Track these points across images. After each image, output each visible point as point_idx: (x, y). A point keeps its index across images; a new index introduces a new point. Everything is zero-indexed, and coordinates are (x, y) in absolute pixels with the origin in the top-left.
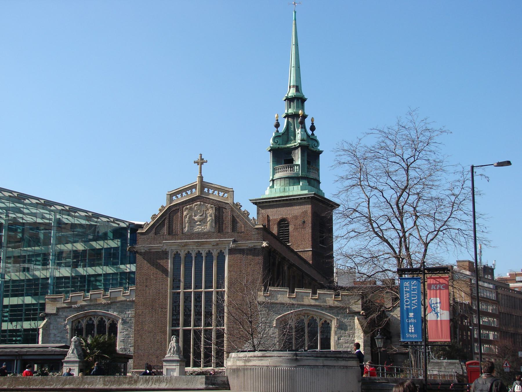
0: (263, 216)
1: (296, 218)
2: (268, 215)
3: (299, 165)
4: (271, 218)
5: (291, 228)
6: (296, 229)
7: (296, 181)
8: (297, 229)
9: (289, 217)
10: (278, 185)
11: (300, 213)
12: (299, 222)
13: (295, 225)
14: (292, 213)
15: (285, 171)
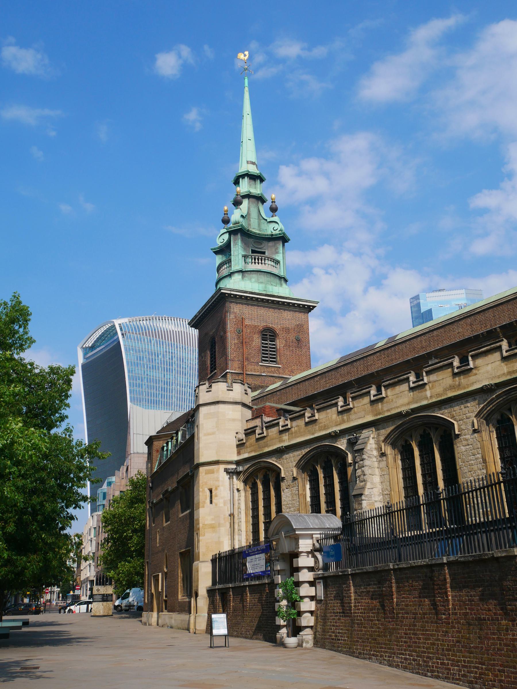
0: (236, 317)
1: (287, 330)
2: (242, 318)
3: (277, 262)
4: (247, 322)
5: (279, 343)
6: (287, 346)
7: (277, 280)
8: (289, 346)
9: (277, 327)
10: (253, 280)
11: (293, 326)
12: (292, 337)
13: (286, 341)
14: (282, 322)
15: (260, 264)
